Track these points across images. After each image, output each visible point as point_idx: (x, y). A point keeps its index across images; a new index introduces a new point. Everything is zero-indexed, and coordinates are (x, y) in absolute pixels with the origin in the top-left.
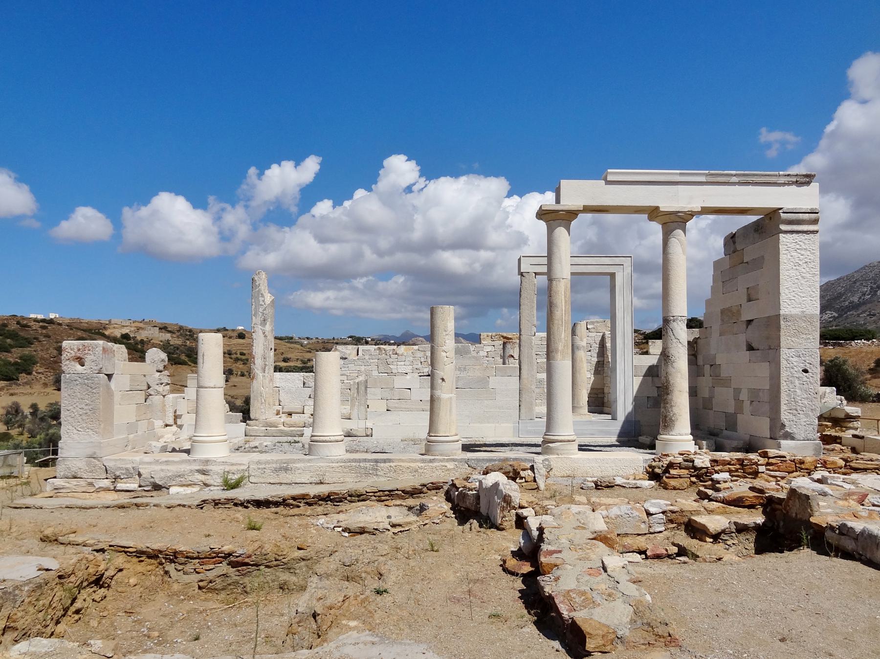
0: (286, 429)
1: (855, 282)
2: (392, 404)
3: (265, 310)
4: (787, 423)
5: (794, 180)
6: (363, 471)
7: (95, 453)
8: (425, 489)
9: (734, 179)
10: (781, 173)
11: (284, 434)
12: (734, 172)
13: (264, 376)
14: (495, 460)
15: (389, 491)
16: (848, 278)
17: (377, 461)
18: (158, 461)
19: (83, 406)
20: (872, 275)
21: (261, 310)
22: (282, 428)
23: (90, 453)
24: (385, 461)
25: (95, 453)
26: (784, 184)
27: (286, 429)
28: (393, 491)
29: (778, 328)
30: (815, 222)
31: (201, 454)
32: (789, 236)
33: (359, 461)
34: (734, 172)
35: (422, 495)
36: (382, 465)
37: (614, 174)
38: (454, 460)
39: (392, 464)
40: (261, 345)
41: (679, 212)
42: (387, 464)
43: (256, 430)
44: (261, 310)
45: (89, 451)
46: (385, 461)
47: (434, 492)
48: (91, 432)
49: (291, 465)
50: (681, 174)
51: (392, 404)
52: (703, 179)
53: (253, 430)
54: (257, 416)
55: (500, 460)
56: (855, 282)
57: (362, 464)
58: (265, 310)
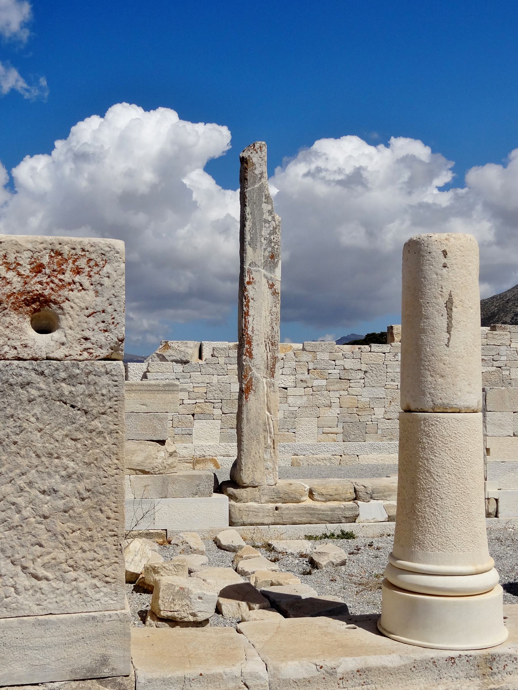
0: (318, 505)
1: (507, 302)
3: (274, 232)
7: (104, 661)
11: (315, 517)
13: (271, 385)
18: (332, 672)
19: (55, 481)
21: (265, 232)
22: (308, 502)
23: (87, 662)
25: (104, 661)
27: (318, 505)
40: (265, 313)
43: (256, 512)
44: (265, 232)
45: (83, 657)
48: (85, 582)
53: (248, 510)
54: (258, 477)
55: (295, 509)
56: (507, 302)
58: (274, 232)
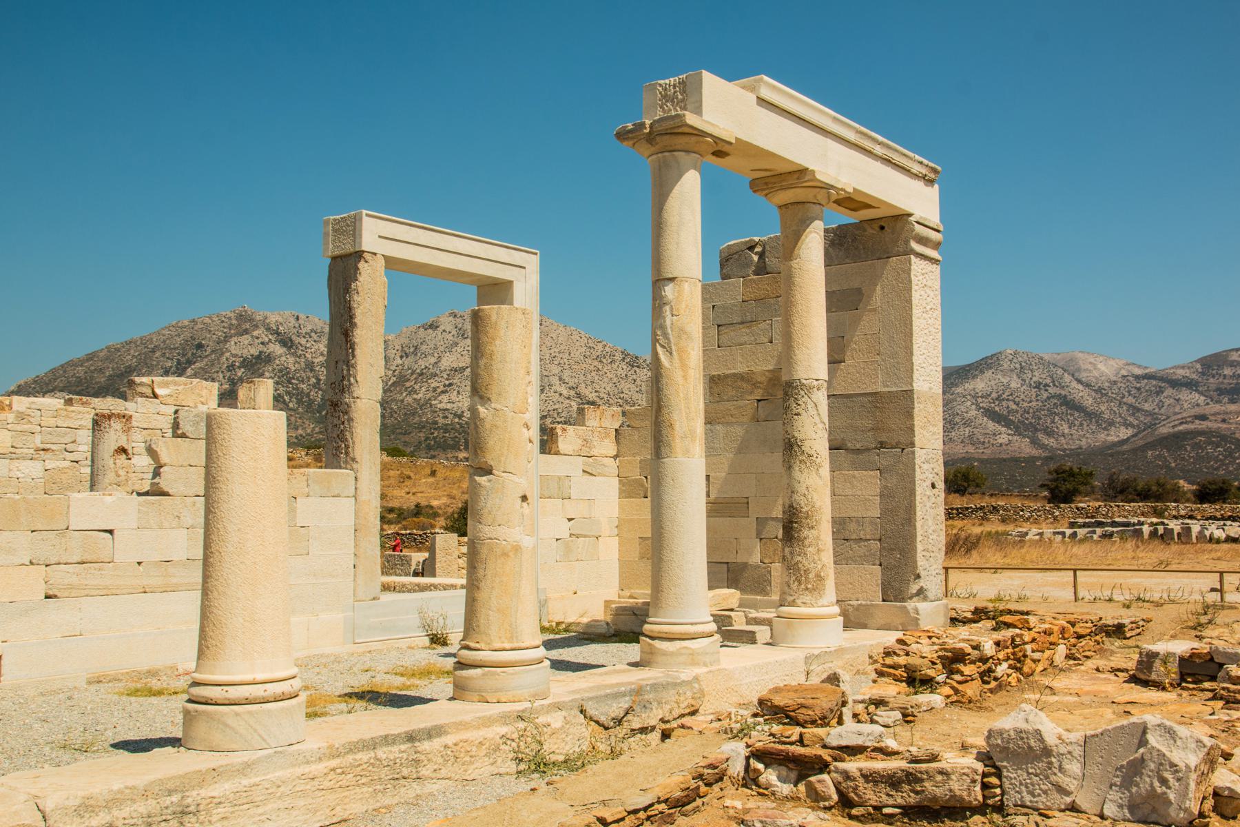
2: (63, 576)
4: (923, 574)
5: (924, 171)
6: (385, 773)
8: (703, 789)
9: (878, 150)
10: (917, 157)
12: (880, 138)
14: (623, 695)
15: (645, 809)
16: (144, 341)
17: (411, 738)
20: (179, 341)
24: (431, 733)
26: (916, 176)
28: (652, 805)
29: (909, 415)
30: (936, 246)
31: (1192, 766)
32: (924, 263)
33: (372, 744)
34: (880, 138)
35: (699, 802)
36: (425, 746)
37: (770, 88)
38: (558, 707)
39: (449, 739)
41: (832, 187)
42: (437, 743)
46: (431, 733)
47: (716, 787)
49: (193, 796)
50: (835, 119)
51: (63, 576)
52: (851, 136)
56: (153, 351)
57: (382, 753)
